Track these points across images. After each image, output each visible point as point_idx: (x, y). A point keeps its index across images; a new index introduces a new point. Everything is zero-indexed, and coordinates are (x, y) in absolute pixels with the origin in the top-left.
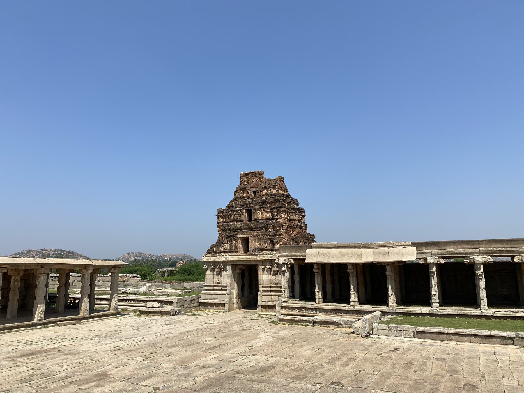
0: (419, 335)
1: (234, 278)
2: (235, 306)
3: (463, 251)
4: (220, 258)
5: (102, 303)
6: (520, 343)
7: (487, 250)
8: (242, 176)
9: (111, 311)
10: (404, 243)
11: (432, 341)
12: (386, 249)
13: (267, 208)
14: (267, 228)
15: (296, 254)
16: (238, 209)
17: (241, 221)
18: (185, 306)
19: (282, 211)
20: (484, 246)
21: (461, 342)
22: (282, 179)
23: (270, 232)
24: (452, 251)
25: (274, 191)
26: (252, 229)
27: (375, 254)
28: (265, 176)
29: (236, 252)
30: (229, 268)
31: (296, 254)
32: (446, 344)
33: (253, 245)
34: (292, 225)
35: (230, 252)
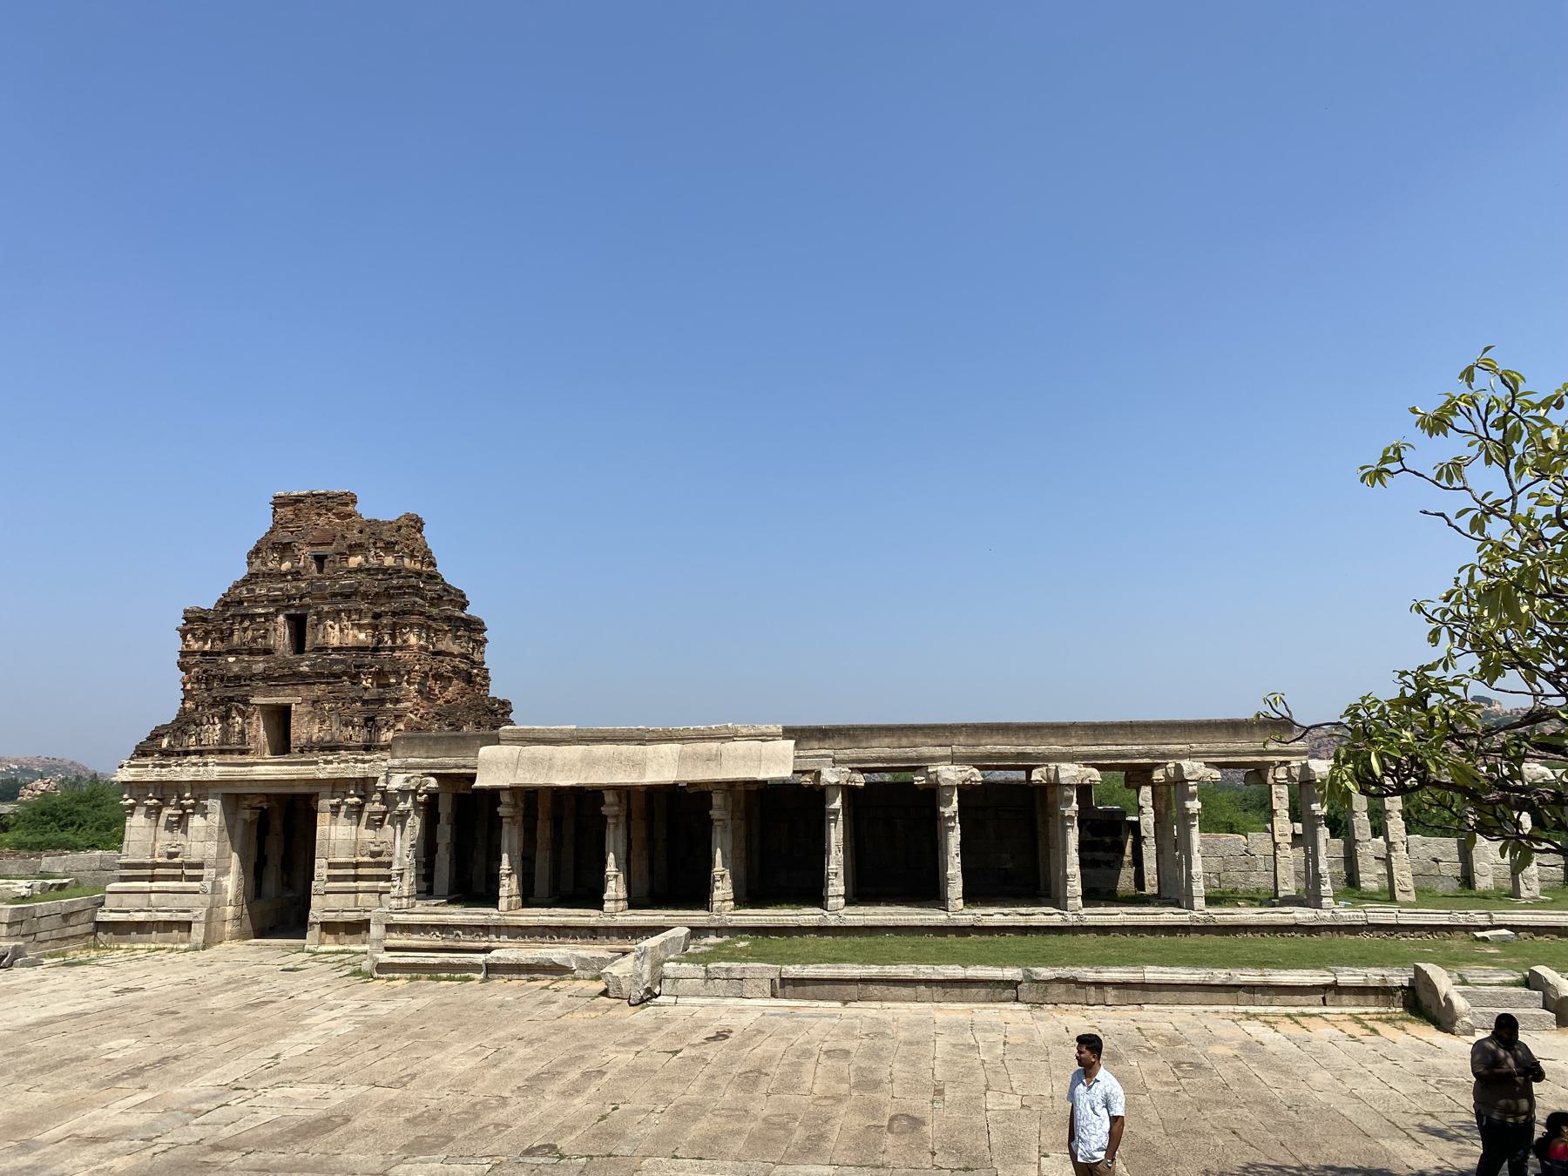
0: (789, 988)
1: (231, 838)
2: (228, 928)
4: (184, 772)
6: (1032, 996)
8: (279, 503)
10: (763, 728)
11: (821, 1004)
12: (714, 745)
13: (360, 612)
14: (355, 679)
15: (447, 760)
16: (260, 611)
17: (268, 651)
18: (41, 936)
19: (412, 626)
20: (962, 739)
22: (417, 524)
23: (366, 689)
25: (389, 561)
27: (682, 759)
28: (358, 508)
29: (243, 752)
30: (214, 805)
31: (447, 760)
32: (856, 1008)
33: (303, 729)
34: (442, 670)
35: (222, 752)
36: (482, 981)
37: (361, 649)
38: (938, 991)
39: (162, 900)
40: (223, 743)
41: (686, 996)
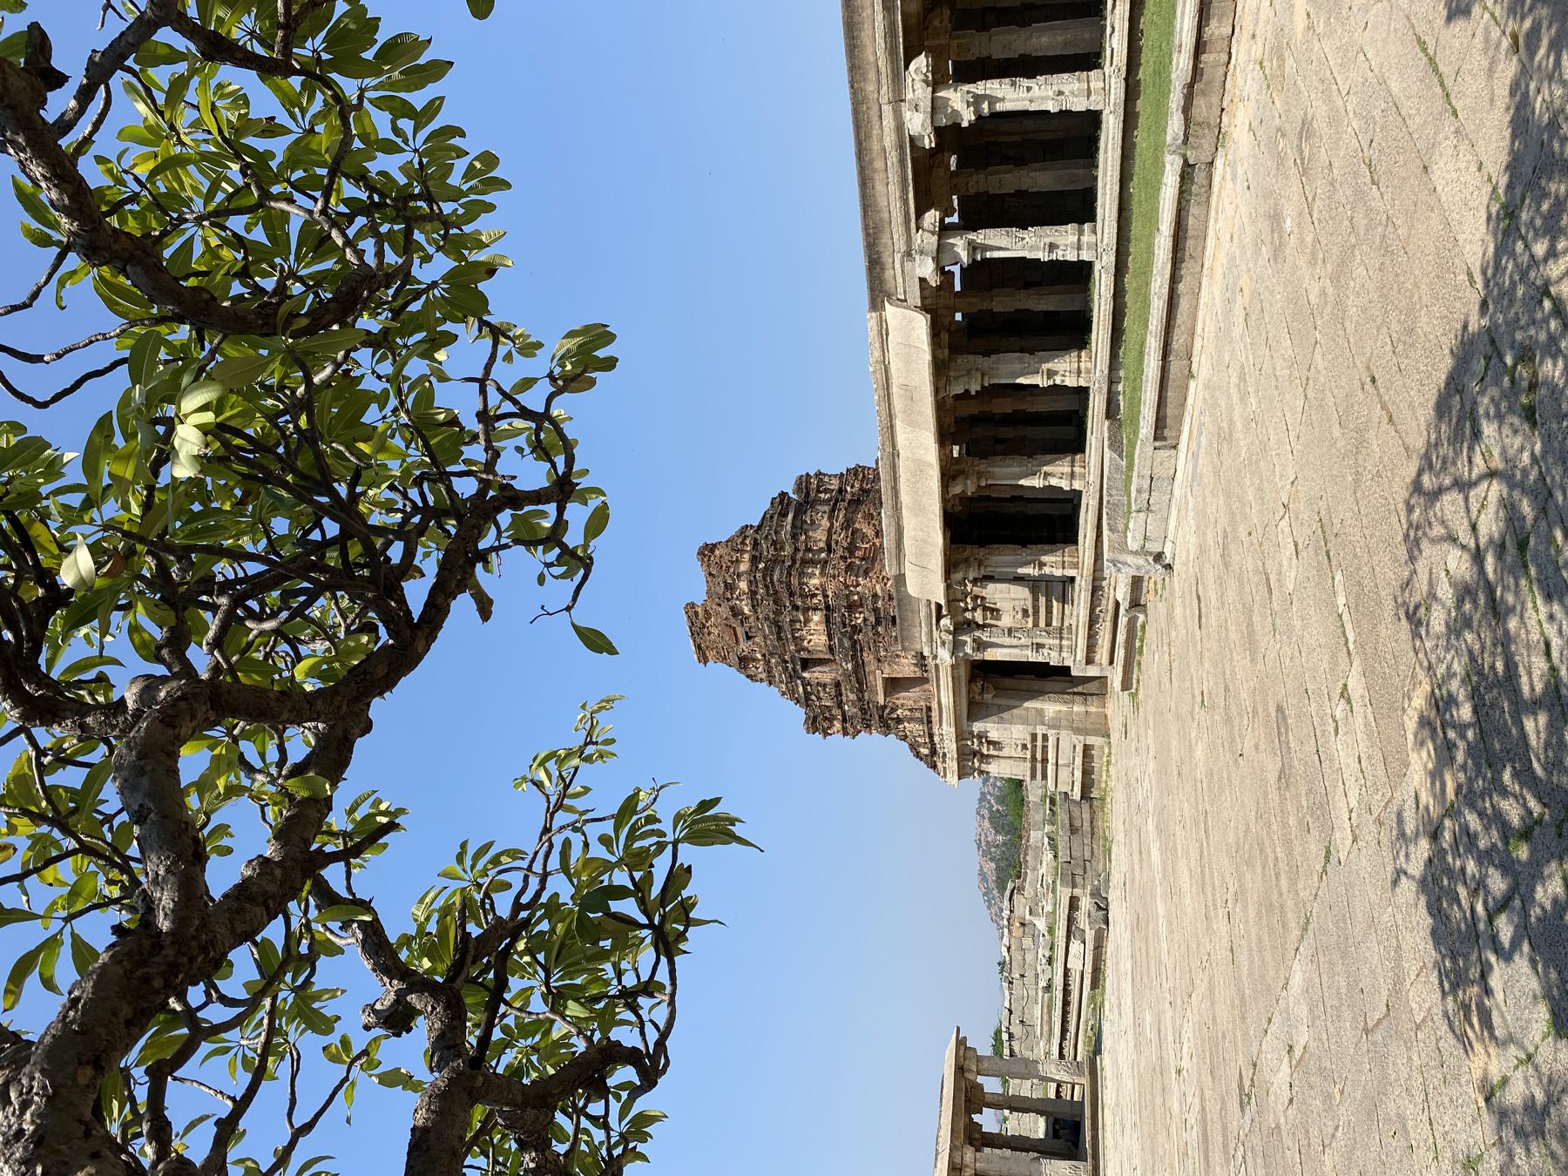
0: (1167, 433)
2: (1093, 709)
3: (893, 157)
4: (949, 746)
5: (1072, 1028)
6: (1207, 143)
7: (884, 81)
8: (704, 659)
9: (1085, 1081)
10: (873, 334)
11: (1190, 401)
12: (895, 389)
13: (793, 622)
14: (856, 629)
15: (922, 614)
17: (837, 685)
18: (1087, 855)
19: (801, 584)
21: (1195, 320)
22: (707, 551)
23: (865, 620)
24: (894, 190)
25: (743, 585)
26: (859, 667)
27: (912, 423)
28: (699, 596)
29: (929, 709)
30: (977, 727)
31: (922, 614)
32: (1203, 363)
35: (929, 722)
36: (1145, 612)
37: (828, 621)
38: (1187, 269)
39: (1067, 747)
40: (921, 721)
41: (1166, 531)
